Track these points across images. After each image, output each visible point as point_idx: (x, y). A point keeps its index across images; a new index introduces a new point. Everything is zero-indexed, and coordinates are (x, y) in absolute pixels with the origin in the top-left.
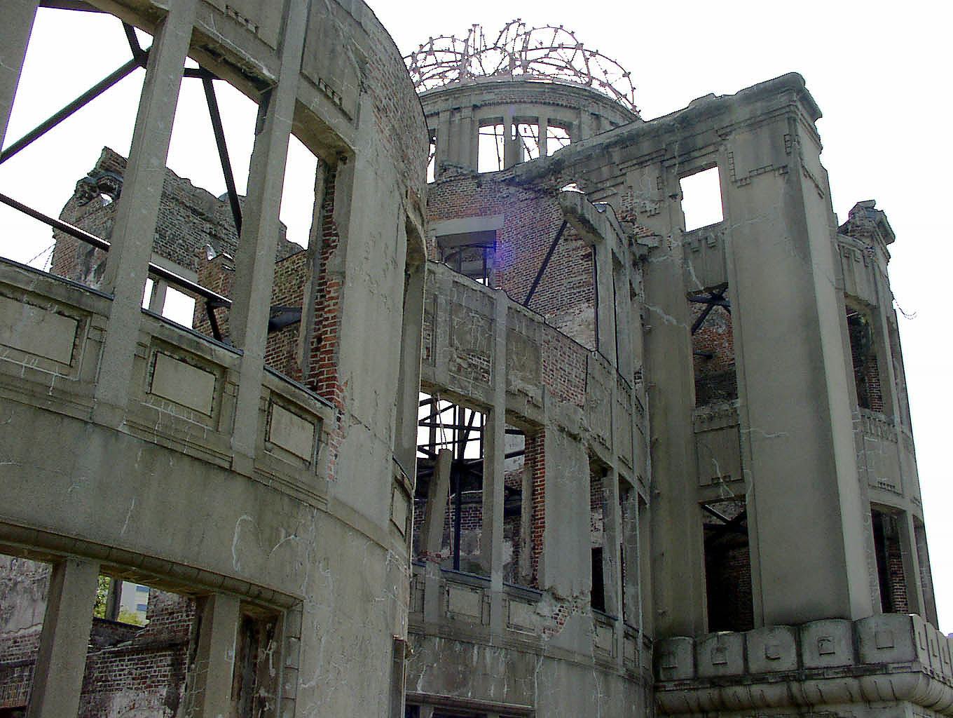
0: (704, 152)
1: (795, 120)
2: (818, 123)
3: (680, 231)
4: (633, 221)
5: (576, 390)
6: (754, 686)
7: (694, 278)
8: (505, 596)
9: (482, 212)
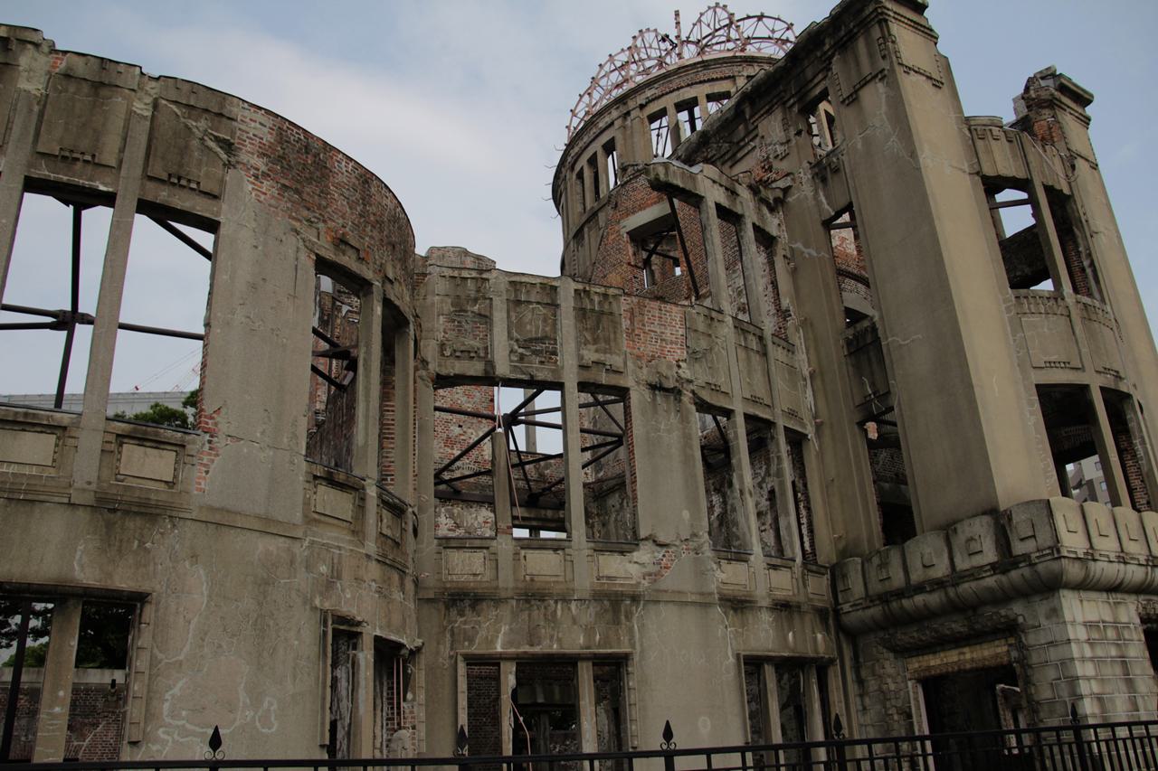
0: (816, 81)
1: (886, 21)
2: (926, 13)
7: (827, 207)
8: (590, 552)
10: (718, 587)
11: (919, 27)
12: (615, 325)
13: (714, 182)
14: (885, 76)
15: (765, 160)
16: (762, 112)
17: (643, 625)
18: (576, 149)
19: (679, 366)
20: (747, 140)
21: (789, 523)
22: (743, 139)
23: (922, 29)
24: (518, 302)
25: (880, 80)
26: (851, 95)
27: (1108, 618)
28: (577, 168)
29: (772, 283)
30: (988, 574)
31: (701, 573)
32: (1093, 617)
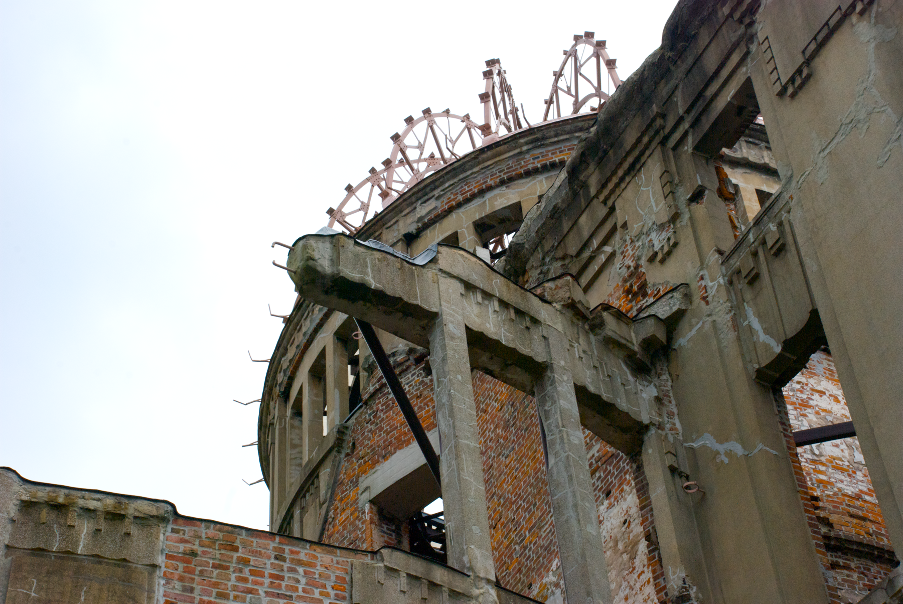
0: (725, 73)
3: (717, 255)
4: (643, 287)
7: (763, 337)
13: (469, 287)
16: (620, 173)
18: (292, 352)
20: (595, 243)
25: (862, 13)
26: (799, 71)
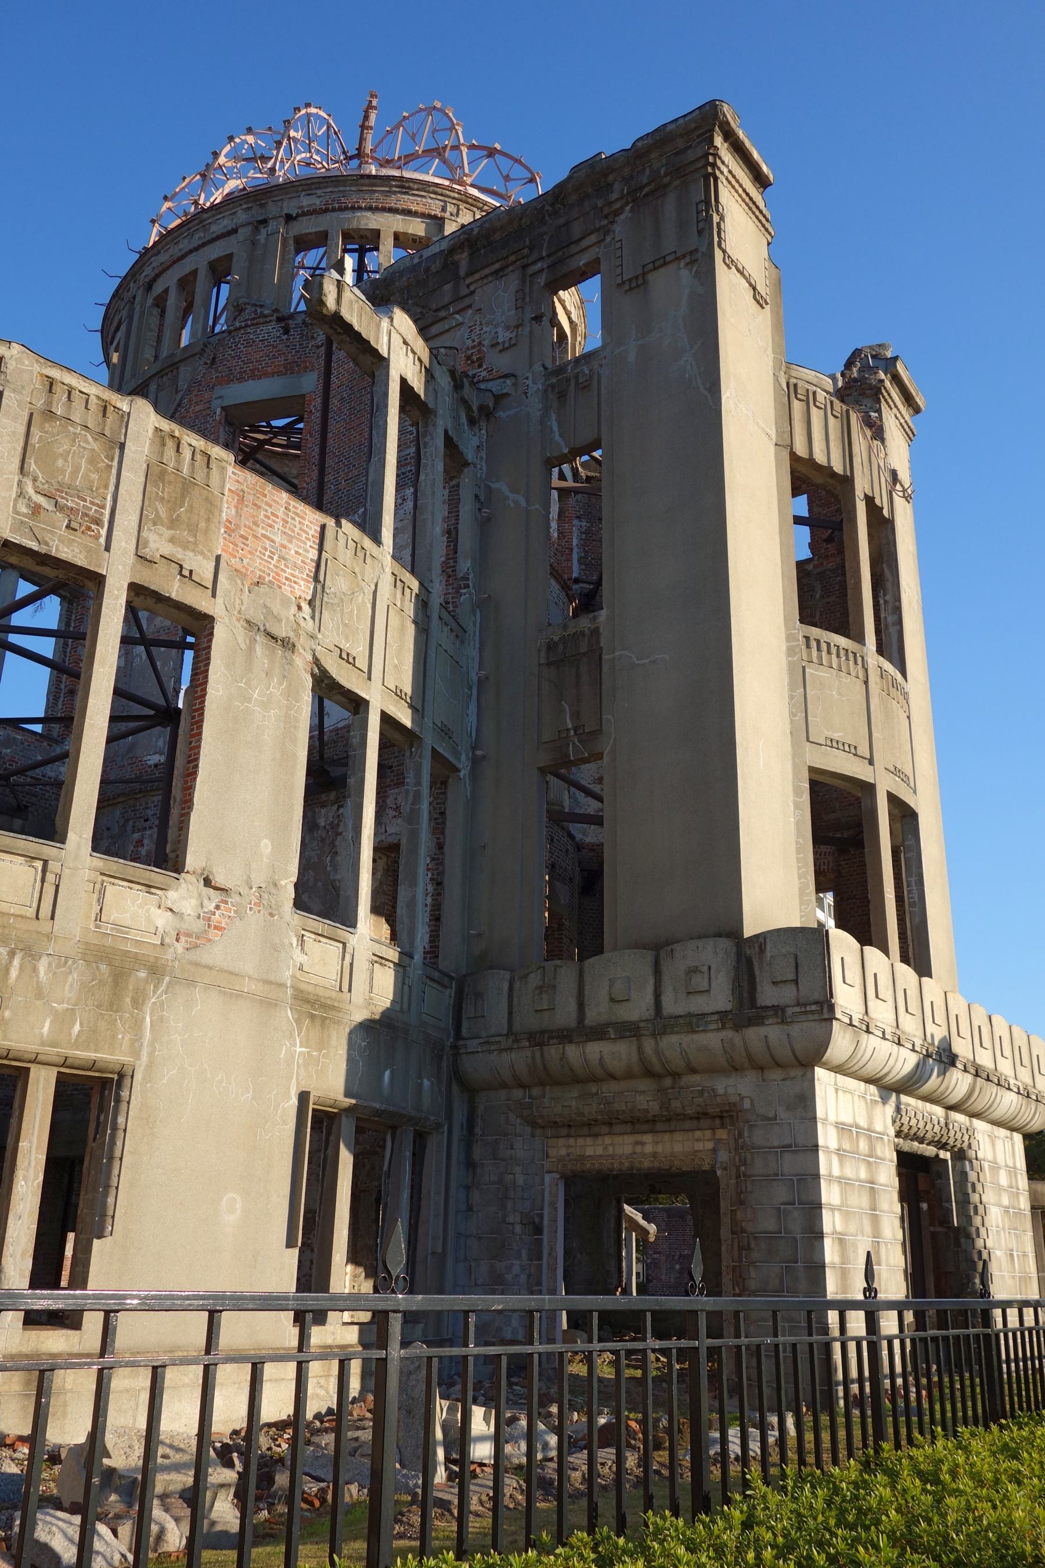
0: (584, 243)
1: (716, 179)
5: (297, 573)
6: (591, 1043)
7: (557, 437)
9: (290, 369)
10: (293, 977)
11: (754, 209)
12: (211, 505)
13: (405, 343)
14: (696, 260)
15: (473, 347)
17: (161, 1019)
18: (164, 258)
19: (300, 608)
21: (414, 897)
22: (446, 307)
23: (757, 213)
24: (49, 414)
25: (687, 264)
26: (637, 277)
27: (863, 1123)
28: (158, 288)
29: (449, 532)
30: (713, 1026)
31: (273, 949)
32: (847, 1118)
